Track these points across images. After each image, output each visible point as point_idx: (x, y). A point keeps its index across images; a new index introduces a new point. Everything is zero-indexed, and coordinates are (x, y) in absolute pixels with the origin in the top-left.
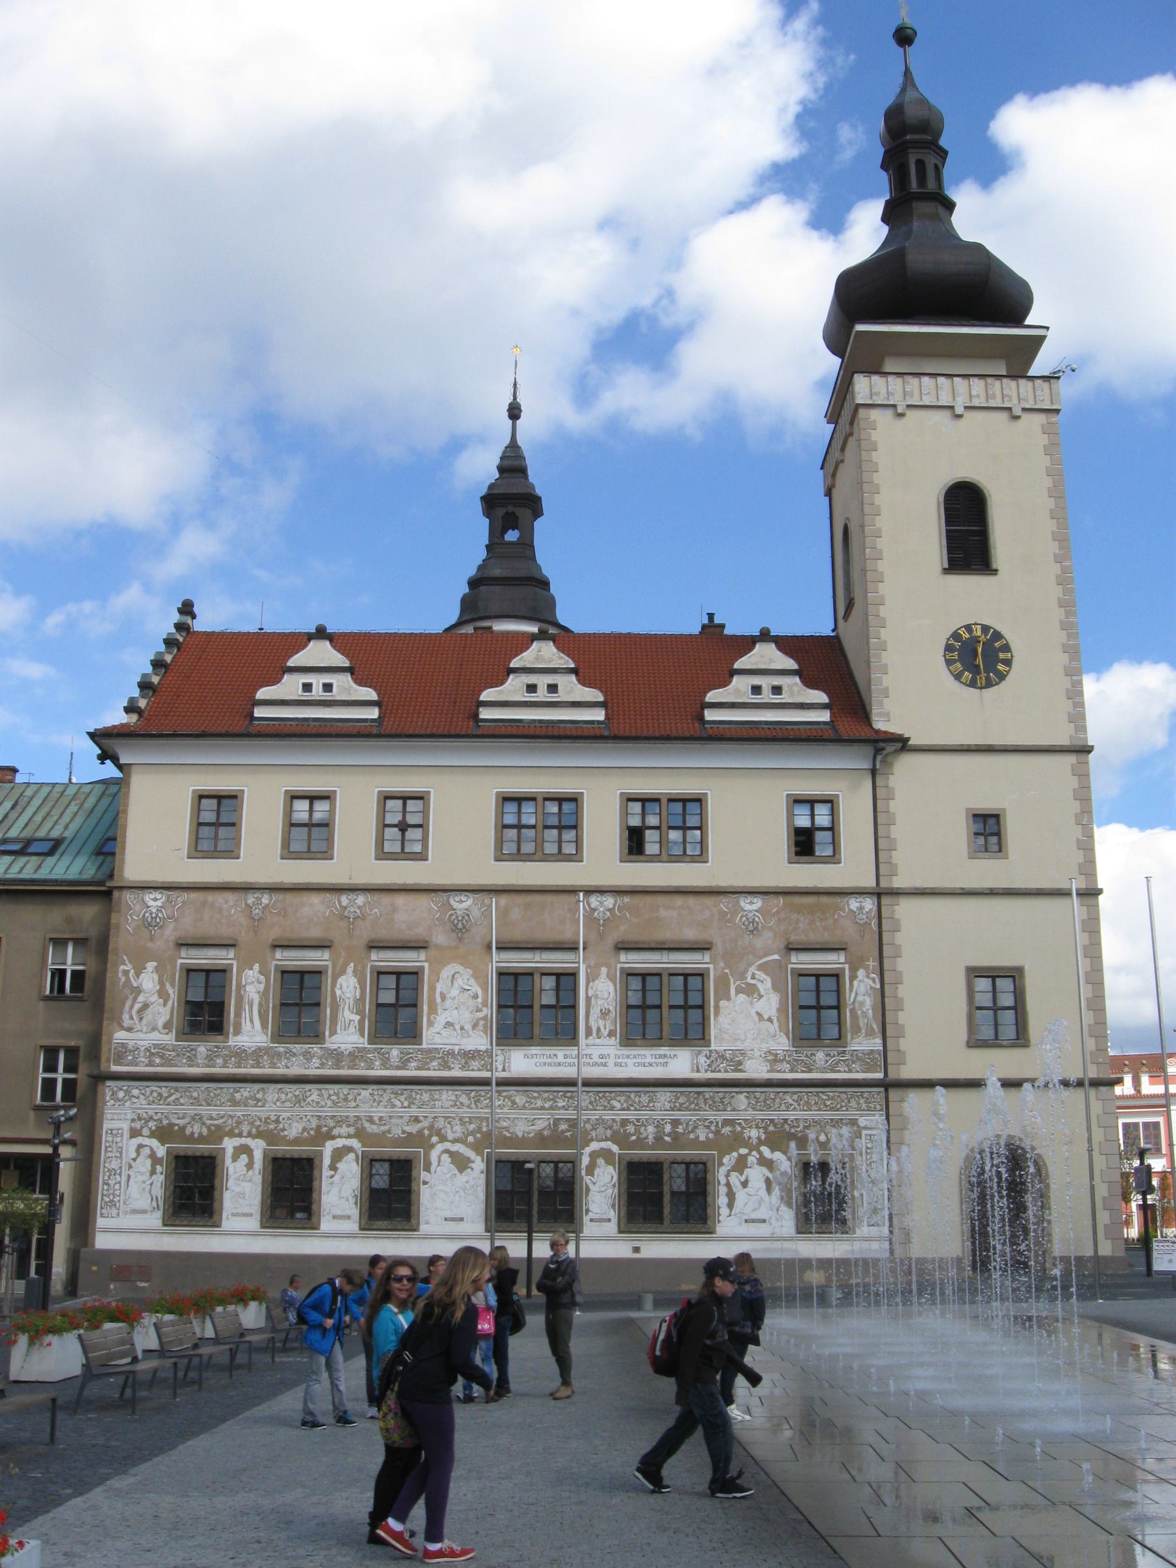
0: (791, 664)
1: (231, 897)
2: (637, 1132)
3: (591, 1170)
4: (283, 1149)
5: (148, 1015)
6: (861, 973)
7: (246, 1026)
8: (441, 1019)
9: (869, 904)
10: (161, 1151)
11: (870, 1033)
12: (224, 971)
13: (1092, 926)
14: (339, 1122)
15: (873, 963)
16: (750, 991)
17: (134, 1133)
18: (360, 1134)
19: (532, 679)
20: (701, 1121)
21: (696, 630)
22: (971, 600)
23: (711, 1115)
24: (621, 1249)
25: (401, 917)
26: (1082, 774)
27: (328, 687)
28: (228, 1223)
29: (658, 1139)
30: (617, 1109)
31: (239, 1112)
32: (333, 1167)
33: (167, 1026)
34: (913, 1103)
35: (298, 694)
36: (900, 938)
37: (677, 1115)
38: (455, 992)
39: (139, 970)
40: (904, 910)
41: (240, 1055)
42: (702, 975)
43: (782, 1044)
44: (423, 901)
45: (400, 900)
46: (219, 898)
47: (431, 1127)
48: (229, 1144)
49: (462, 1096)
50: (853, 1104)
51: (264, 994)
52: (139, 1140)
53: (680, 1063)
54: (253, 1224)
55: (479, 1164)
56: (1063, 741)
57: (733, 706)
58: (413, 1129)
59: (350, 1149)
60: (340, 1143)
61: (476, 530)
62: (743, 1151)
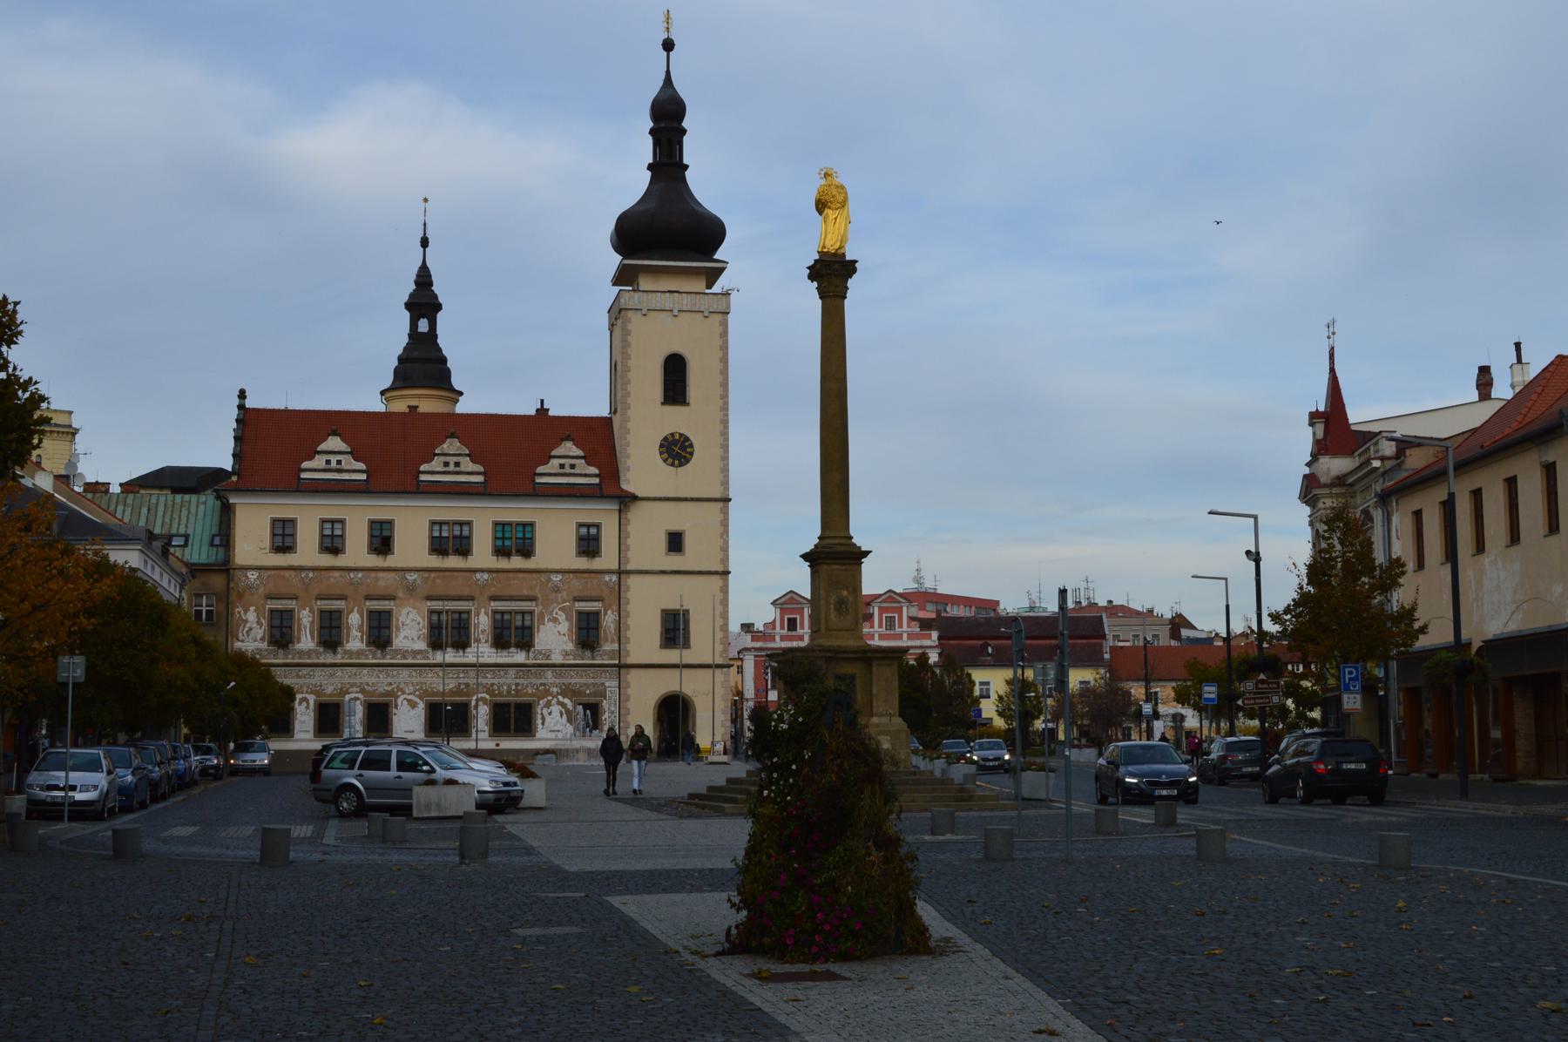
0: (580, 453)
1: (293, 573)
3: (476, 707)
5: (252, 633)
7: (303, 639)
8: (402, 635)
9: (614, 578)
12: (291, 611)
13: (725, 590)
15: (615, 607)
16: (555, 620)
18: (362, 691)
19: (448, 459)
20: (529, 684)
21: (533, 413)
22: (675, 420)
23: (534, 681)
24: (489, 745)
25: (381, 583)
26: (725, 513)
27: (339, 462)
30: (488, 679)
31: (301, 681)
33: (262, 639)
34: (633, 676)
35: (323, 465)
36: (629, 595)
39: (246, 611)
40: (633, 581)
41: (301, 653)
42: (531, 613)
43: (570, 646)
44: (392, 574)
45: (380, 575)
46: (287, 573)
49: (413, 672)
51: (312, 623)
53: (519, 657)
54: (310, 735)
55: (421, 705)
56: (717, 495)
57: (550, 475)
59: (357, 699)
61: (401, 322)
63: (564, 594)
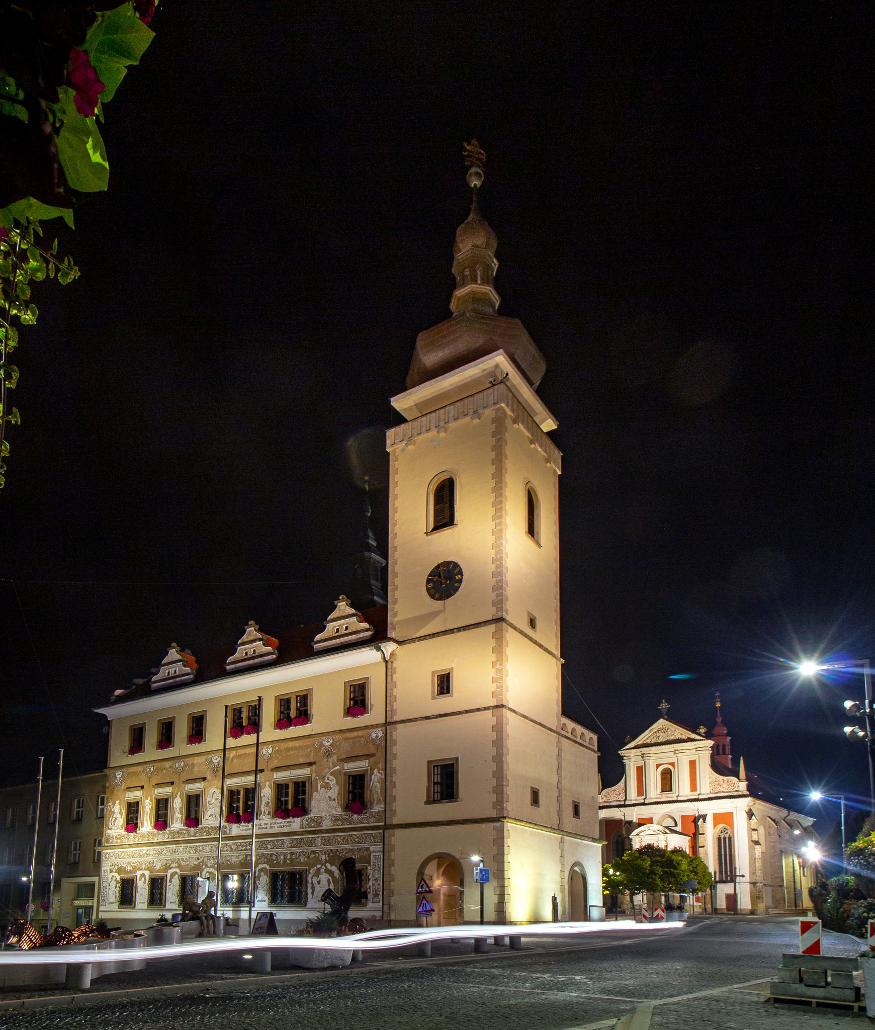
2: (277, 859)
4: (155, 874)
6: (376, 771)
8: (209, 812)
10: (118, 879)
11: (379, 802)
14: (173, 862)
15: (381, 765)
16: (327, 786)
17: (111, 871)
18: (179, 866)
28: (138, 906)
29: (285, 862)
31: (141, 859)
32: (170, 881)
37: (293, 850)
38: (213, 801)
43: (339, 812)
45: (197, 760)
47: (202, 862)
48: (139, 873)
50: (368, 840)
51: (151, 809)
52: (113, 874)
53: (296, 824)
54: (145, 906)
58: (196, 863)
59: (176, 873)
60: (173, 870)
62: (319, 866)
63: (335, 758)
